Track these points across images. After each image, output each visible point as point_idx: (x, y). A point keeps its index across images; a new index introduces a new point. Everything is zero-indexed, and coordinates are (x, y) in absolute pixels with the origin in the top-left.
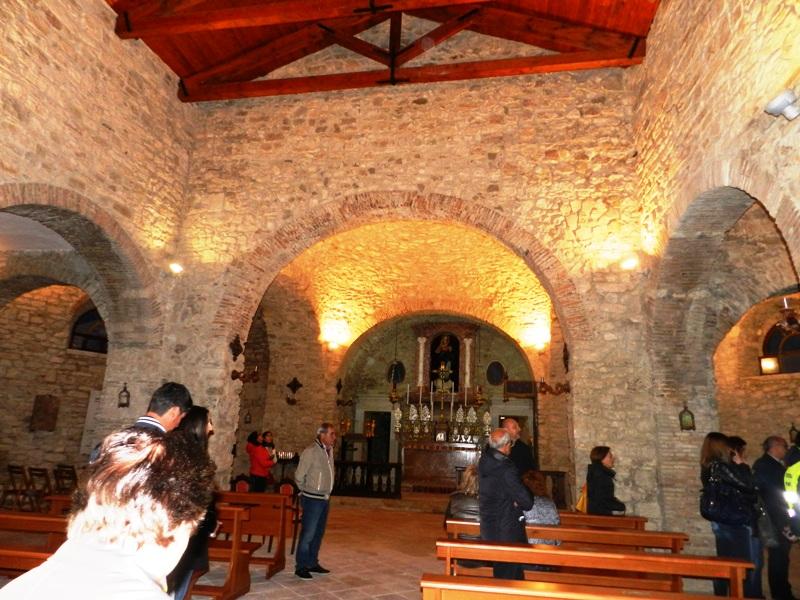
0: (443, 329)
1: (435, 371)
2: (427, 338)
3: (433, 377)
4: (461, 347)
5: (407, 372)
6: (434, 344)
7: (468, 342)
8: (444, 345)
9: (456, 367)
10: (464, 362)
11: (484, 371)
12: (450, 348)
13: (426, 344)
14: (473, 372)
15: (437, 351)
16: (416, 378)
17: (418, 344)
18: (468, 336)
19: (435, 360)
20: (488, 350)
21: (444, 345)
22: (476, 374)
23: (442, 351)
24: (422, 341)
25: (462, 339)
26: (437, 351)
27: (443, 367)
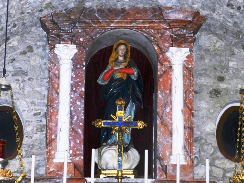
0: (114, 26)
1: (101, 124)
2: (79, 45)
3: (93, 138)
4: (160, 70)
5: (27, 130)
6: (94, 64)
7: (177, 56)
8: (119, 67)
9: (147, 110)
10: (168, 103)
11: (211, 127)
12: (135, 73)
13: (76, 61)
14: (189, 128)
15: (101, 81)
16: (50, 142)
17: (54, 61)
18: (178, 41)
19: (96, 103)
20: (221, 79)
21: (119, 67)
22: (197, 133)
23: (112, 80)
24: (66, 52)
25: (163, 51)
26: (101, 81)
27: (120, 113)
